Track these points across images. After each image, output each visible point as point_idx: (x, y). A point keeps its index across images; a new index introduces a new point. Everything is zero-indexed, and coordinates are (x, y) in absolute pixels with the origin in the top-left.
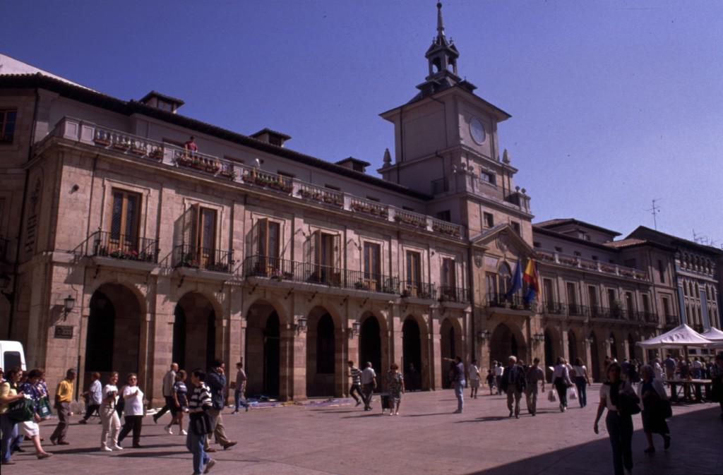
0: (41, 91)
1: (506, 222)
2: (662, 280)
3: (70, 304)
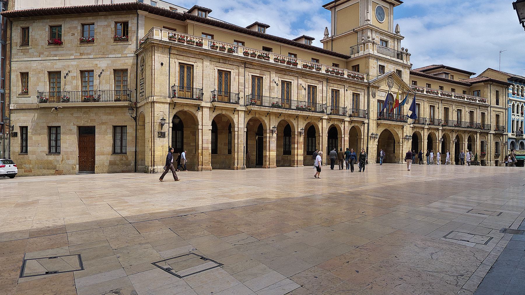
0: (139, 11)
1: (392, 70)
2: (497, 103)
3: (163, 122)
